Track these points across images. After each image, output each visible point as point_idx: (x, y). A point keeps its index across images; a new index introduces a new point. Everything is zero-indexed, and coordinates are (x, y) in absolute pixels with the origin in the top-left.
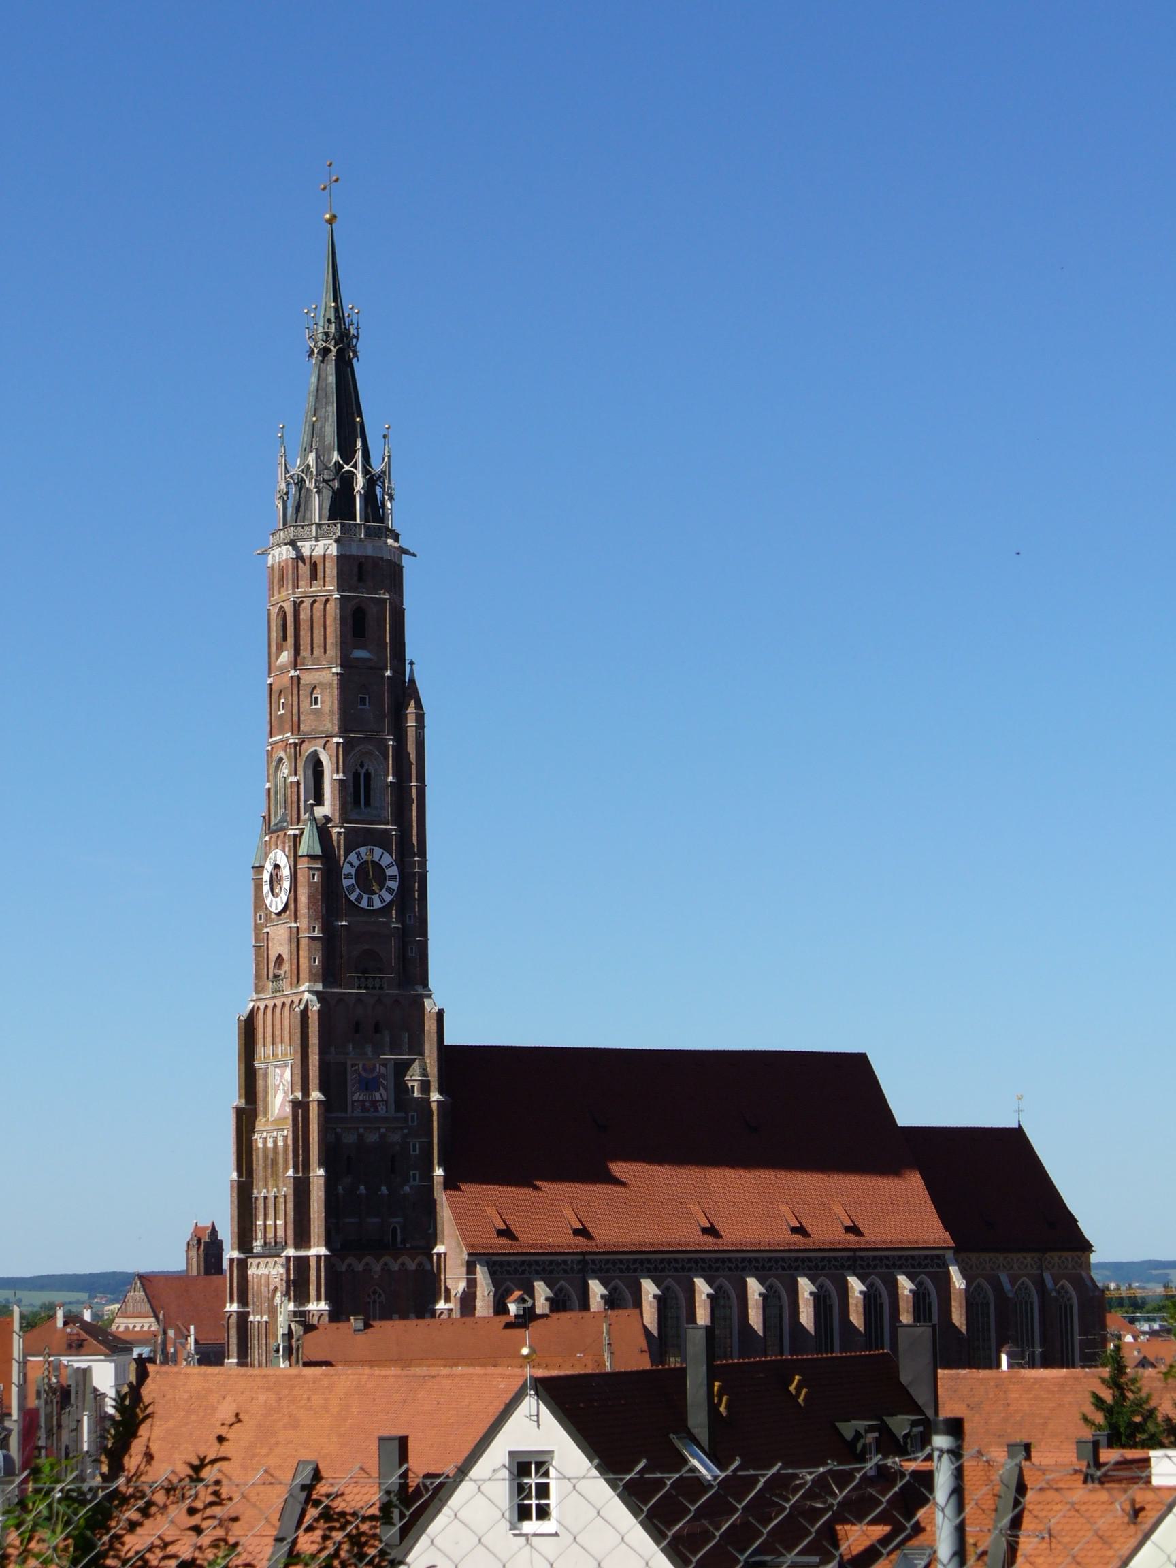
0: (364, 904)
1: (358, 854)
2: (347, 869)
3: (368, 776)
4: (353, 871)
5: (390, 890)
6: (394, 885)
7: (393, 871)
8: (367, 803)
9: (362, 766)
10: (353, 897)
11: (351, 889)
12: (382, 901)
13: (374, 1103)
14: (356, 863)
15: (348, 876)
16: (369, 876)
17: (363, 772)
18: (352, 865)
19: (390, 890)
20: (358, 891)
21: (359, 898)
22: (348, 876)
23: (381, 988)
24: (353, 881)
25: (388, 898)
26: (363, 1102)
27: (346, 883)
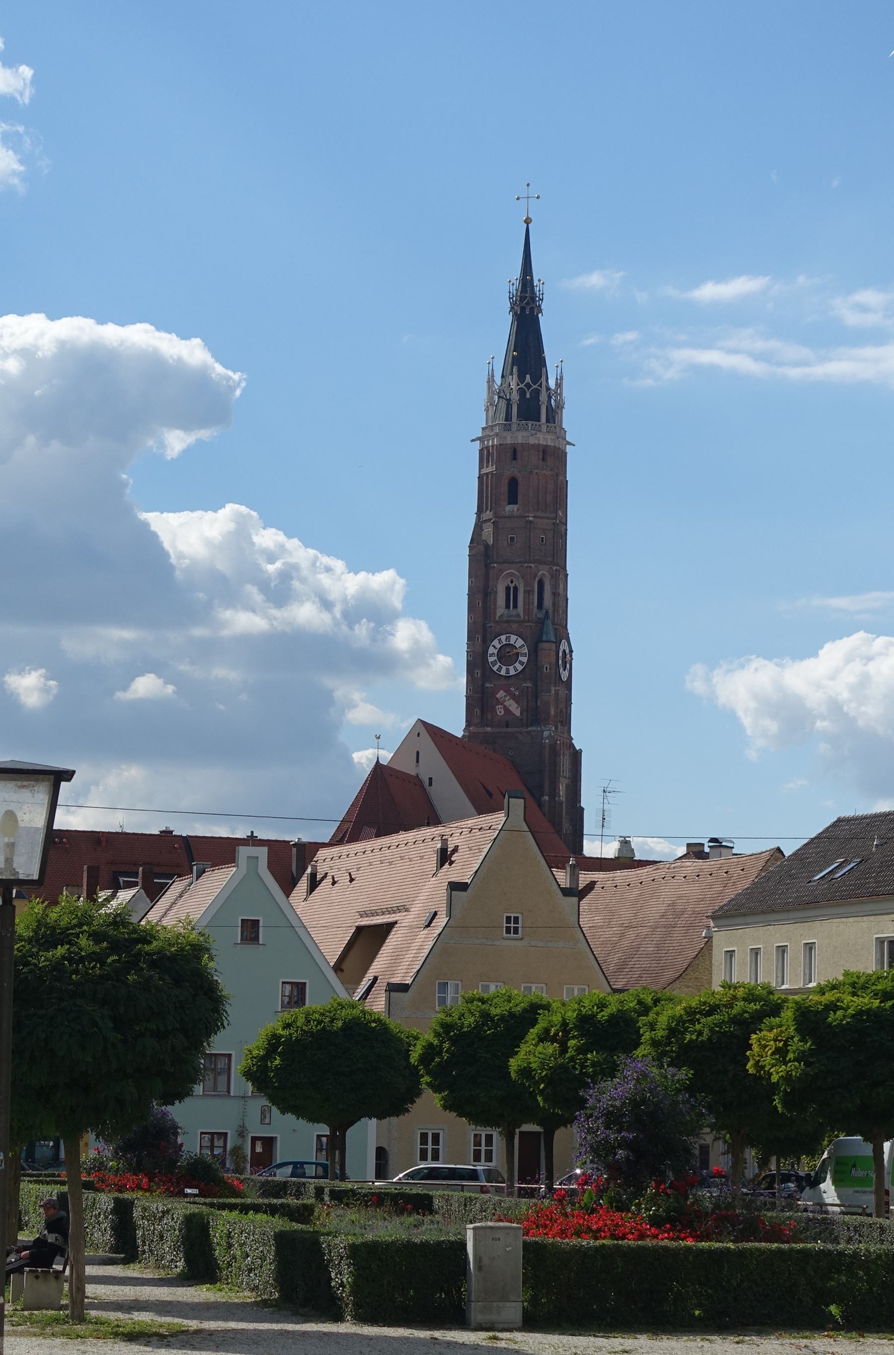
0: (503, 673)
1: (500, 640)
2: (491, 650)
3: (516, 589)
4: (496, 651)
5: (521, 663)
6: (525, 659)
9: (512, 582)
10: (495, 669)
12: (516, 670)
14: (498, 646)
15: (491, 655)
16: (507, 655)
17: (512, 586)
19: (521, 663)
20: (499, 664)
22: (491, 655)
25: (520, 668)
27: (491, 659)
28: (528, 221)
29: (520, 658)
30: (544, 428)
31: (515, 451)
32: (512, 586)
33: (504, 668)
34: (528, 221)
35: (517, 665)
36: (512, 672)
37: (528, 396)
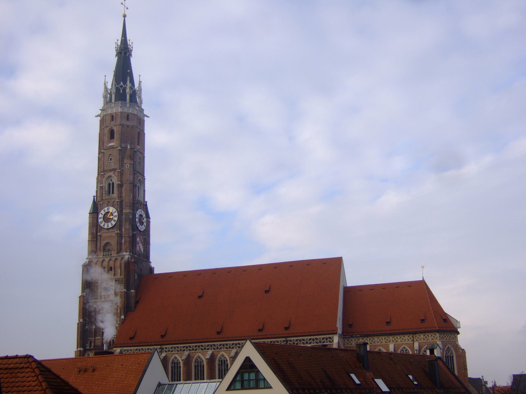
0: (106, 227)
1: (104, 211)
2: (100, 216)
3: (113, 184)
4: (102, 216)
5: (115, 221)
7: (116, 214)
8: (113, 193)
10: (102, 225)
13: (108, 296)
14: (104, 213)
15: (100, 218)
19: (115, 221)
22: (100, 218)
24: (102, 220)
25: (114, 223)
26: (105, 295)
27: (100, 220)
28: (125, 16)
30: (128, 105)
31: (113, 116)
33: (106, 224)
34: (125, 16)
37: (121, 92)
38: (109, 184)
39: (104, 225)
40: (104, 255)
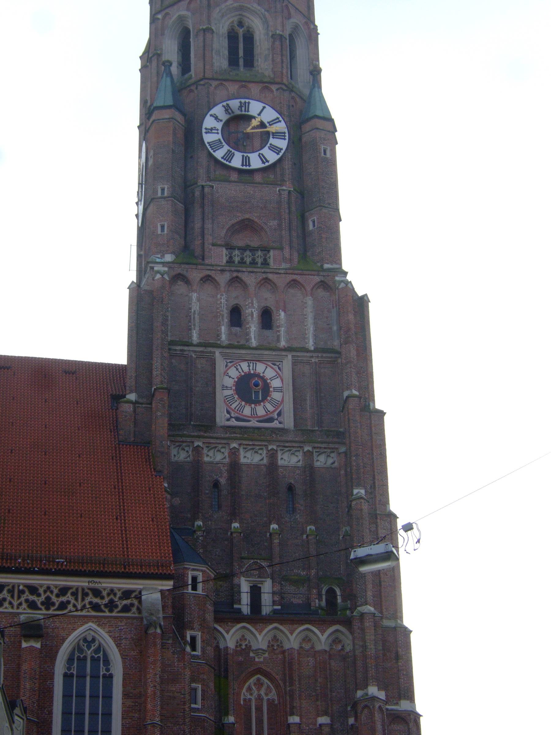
0: (236, 162)
2: (209, 122)
4: (219, 126)
5: (275, 149)
6: (283, 144)
10: (219, 154)
11: (217, 145)
15: (210, 131)
17: (241, 32)
18: (216, 118)
19: (275, 149)
20: (226, 148)
21: (229, 156)
22: (210, 131)
23: (265, 263)
24: (219, 136)
25: (272, 157)
27: (208, 138)
29: (272, 141)
32: (241, 32)
35: (266, 151)
36: (256, 163)
38: (232, 37)
39: (229, 156)
40: (230, 261)
